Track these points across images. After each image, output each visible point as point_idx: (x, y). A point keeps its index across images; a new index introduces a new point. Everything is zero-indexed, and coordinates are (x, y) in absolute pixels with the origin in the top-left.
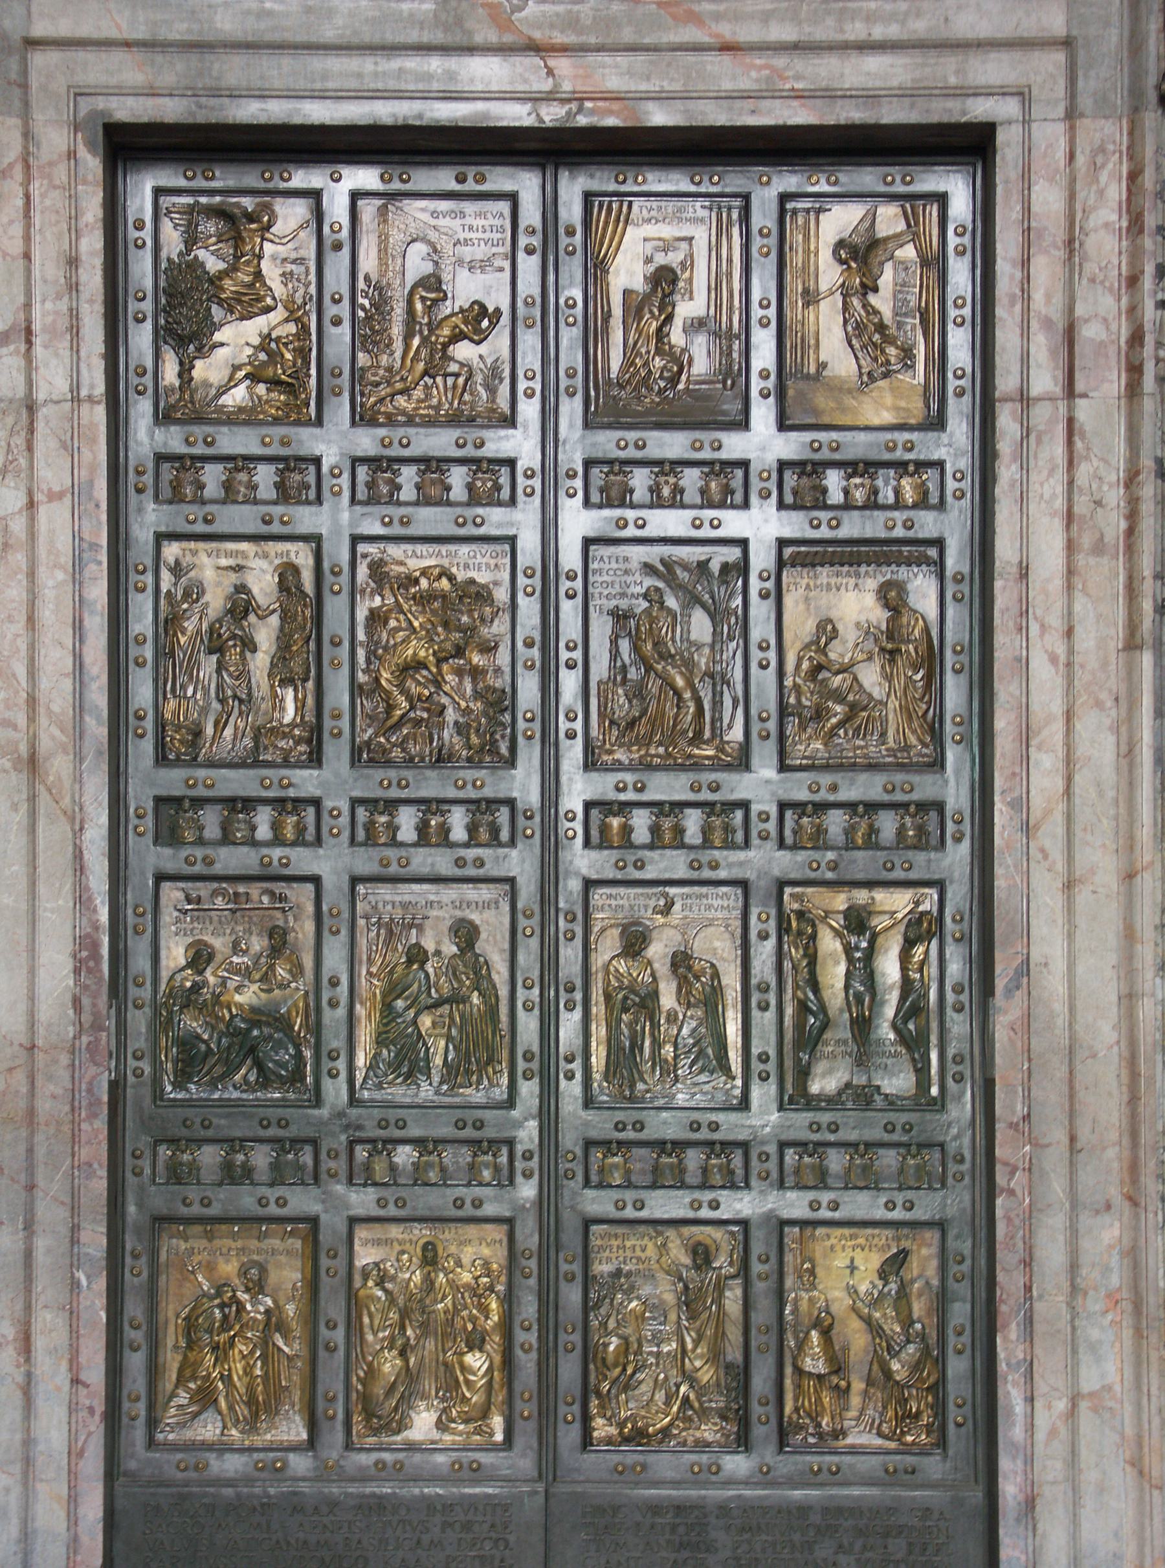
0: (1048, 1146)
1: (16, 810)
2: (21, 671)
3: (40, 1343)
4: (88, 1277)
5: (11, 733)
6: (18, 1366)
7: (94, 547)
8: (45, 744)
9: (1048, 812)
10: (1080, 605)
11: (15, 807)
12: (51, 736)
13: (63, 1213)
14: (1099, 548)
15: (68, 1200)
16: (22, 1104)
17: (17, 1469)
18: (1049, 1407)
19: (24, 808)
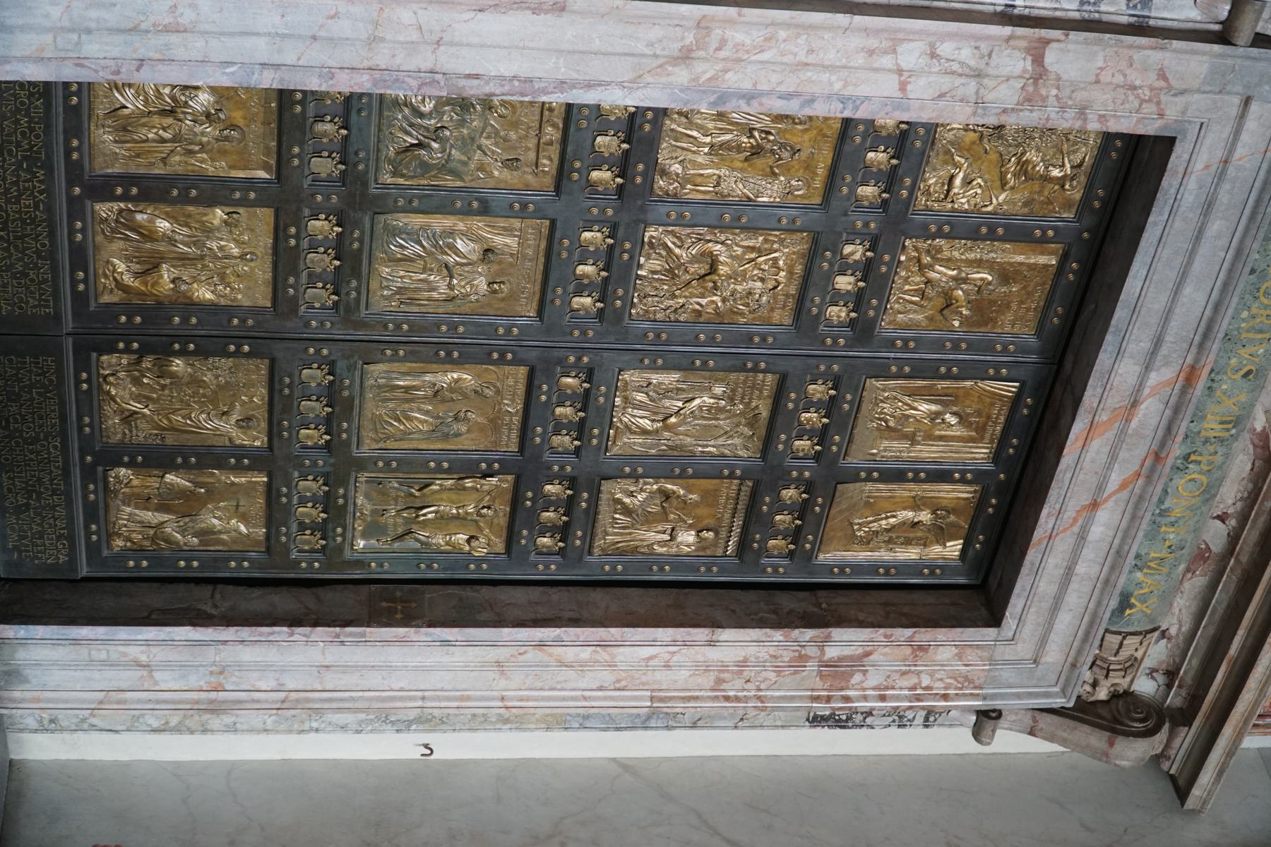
0: (324, 654)
1: (647, 46)
2: (765, 56)
3: (174, 38)
4: (232, 73)
5: (714, 45)
6: (154, 25)
7: (856, 108)
8: (699, 67)
9: (551, 655)
10: (685, 673)
11: (650, 44)
12: (705, 70)
13: (290, 59)
14: (720, 681)
15: (301, 63)
16: (388, 37)
17: (65, 23)
18: (142, 652)
19: (648, 51)
